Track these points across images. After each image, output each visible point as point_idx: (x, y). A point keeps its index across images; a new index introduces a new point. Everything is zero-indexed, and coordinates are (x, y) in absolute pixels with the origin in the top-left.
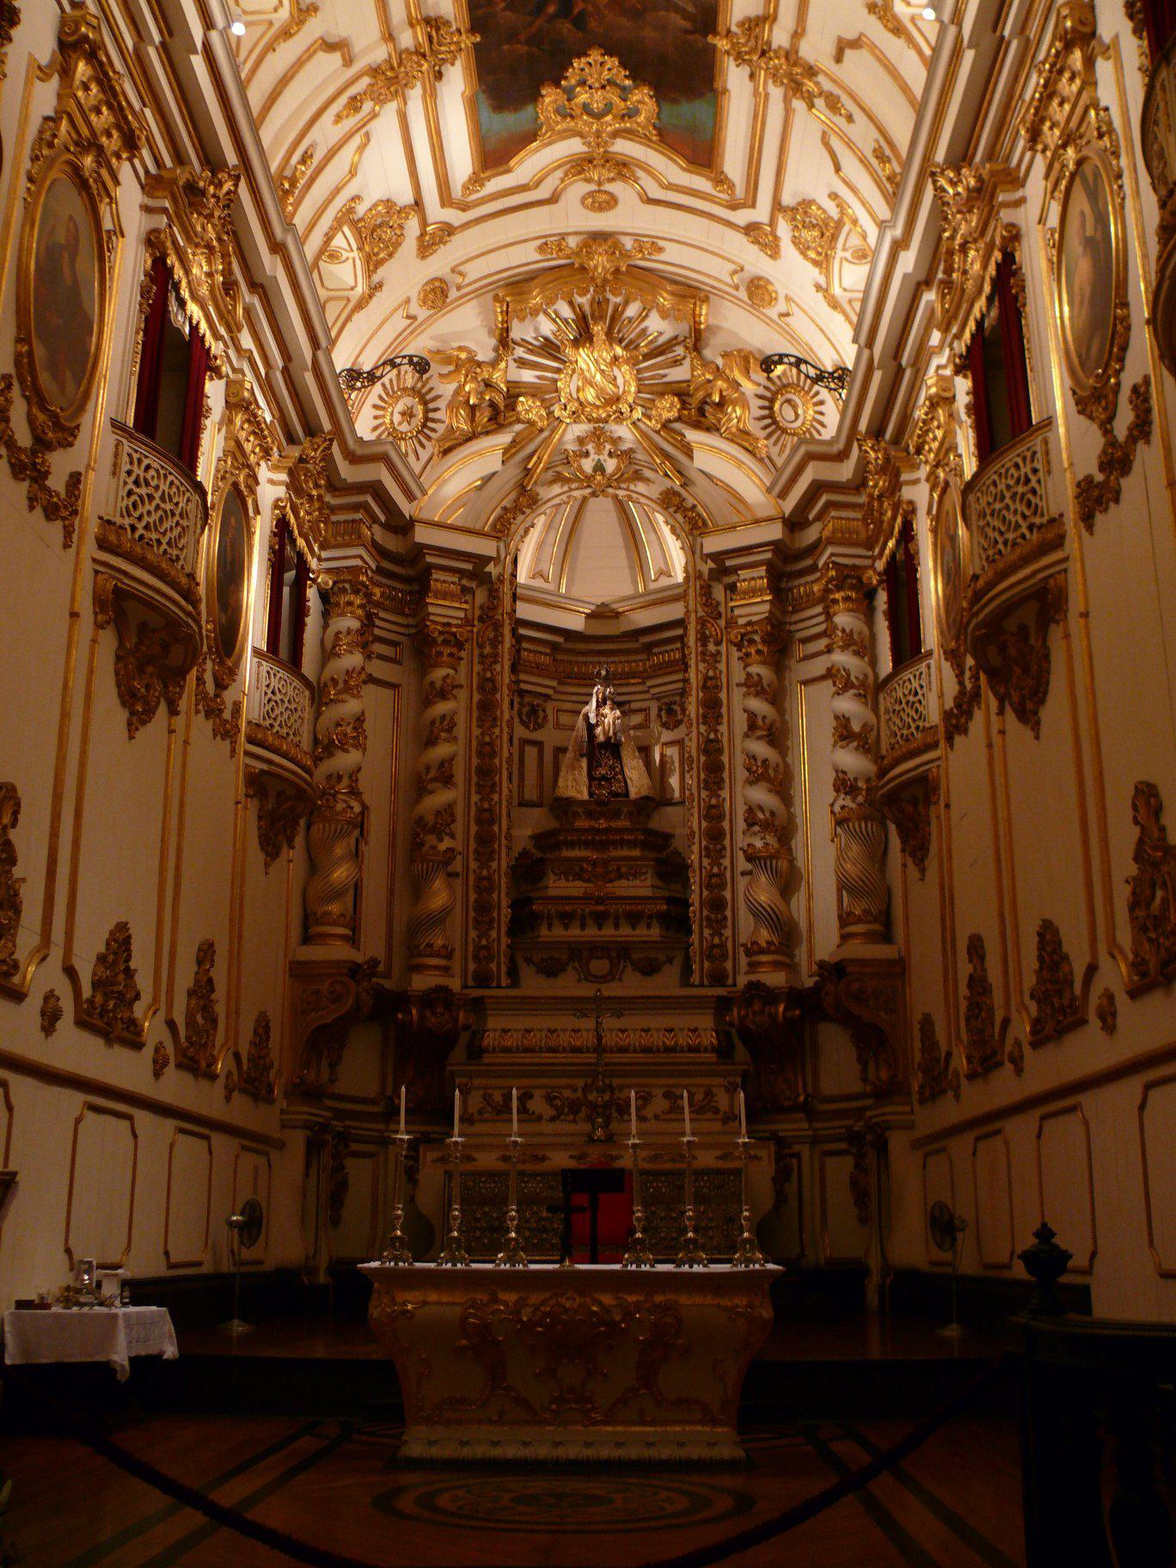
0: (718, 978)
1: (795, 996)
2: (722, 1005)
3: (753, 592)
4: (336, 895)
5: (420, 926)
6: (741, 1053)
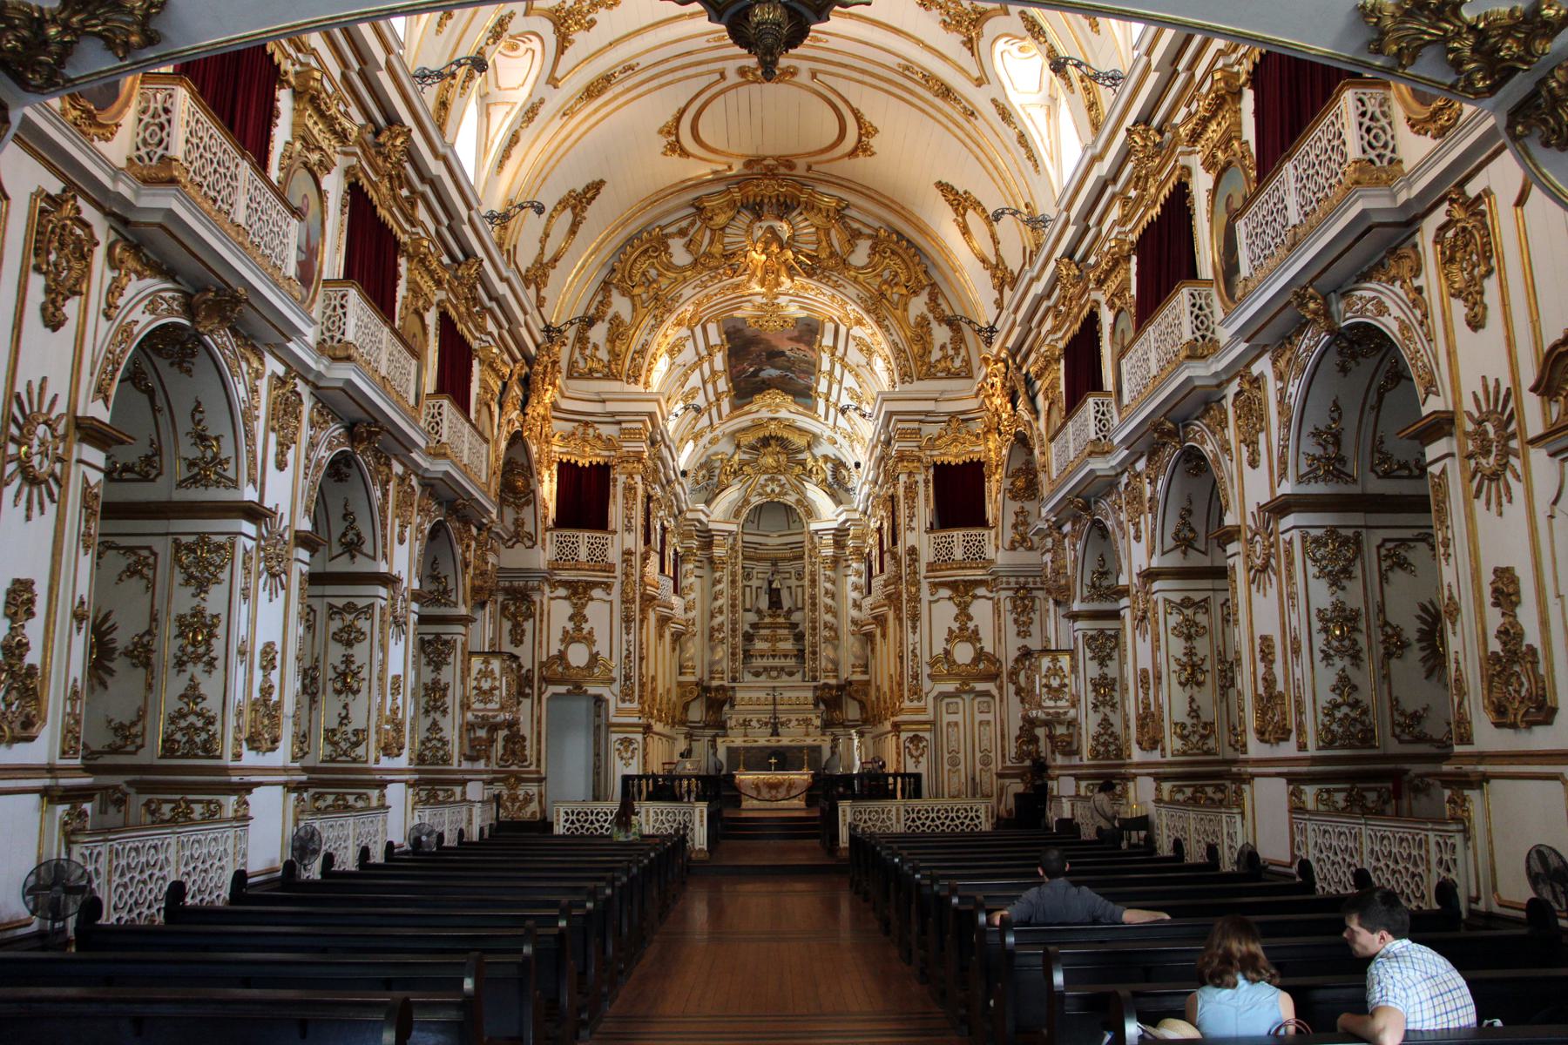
0: (814, 679)
1: (840, 688)
2: (815, 687)
3: (827, 546)
4: (689, 659)
5: (712, 664)
6: (822, 707)
